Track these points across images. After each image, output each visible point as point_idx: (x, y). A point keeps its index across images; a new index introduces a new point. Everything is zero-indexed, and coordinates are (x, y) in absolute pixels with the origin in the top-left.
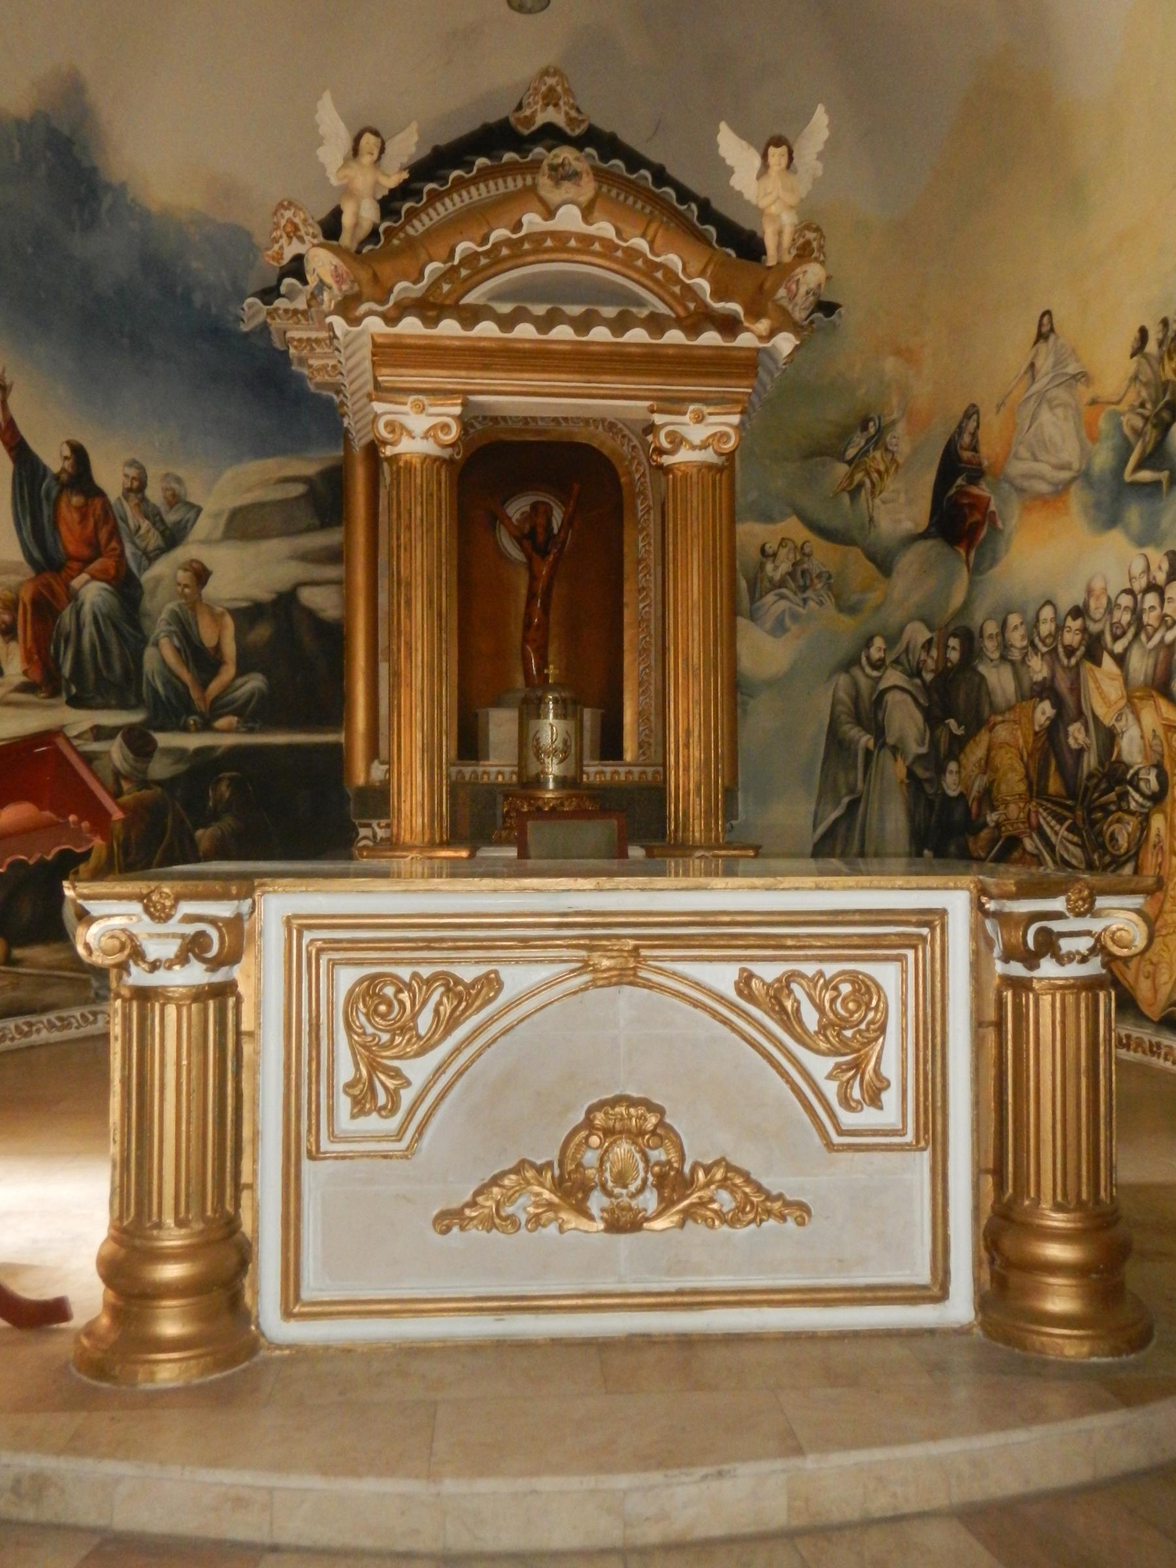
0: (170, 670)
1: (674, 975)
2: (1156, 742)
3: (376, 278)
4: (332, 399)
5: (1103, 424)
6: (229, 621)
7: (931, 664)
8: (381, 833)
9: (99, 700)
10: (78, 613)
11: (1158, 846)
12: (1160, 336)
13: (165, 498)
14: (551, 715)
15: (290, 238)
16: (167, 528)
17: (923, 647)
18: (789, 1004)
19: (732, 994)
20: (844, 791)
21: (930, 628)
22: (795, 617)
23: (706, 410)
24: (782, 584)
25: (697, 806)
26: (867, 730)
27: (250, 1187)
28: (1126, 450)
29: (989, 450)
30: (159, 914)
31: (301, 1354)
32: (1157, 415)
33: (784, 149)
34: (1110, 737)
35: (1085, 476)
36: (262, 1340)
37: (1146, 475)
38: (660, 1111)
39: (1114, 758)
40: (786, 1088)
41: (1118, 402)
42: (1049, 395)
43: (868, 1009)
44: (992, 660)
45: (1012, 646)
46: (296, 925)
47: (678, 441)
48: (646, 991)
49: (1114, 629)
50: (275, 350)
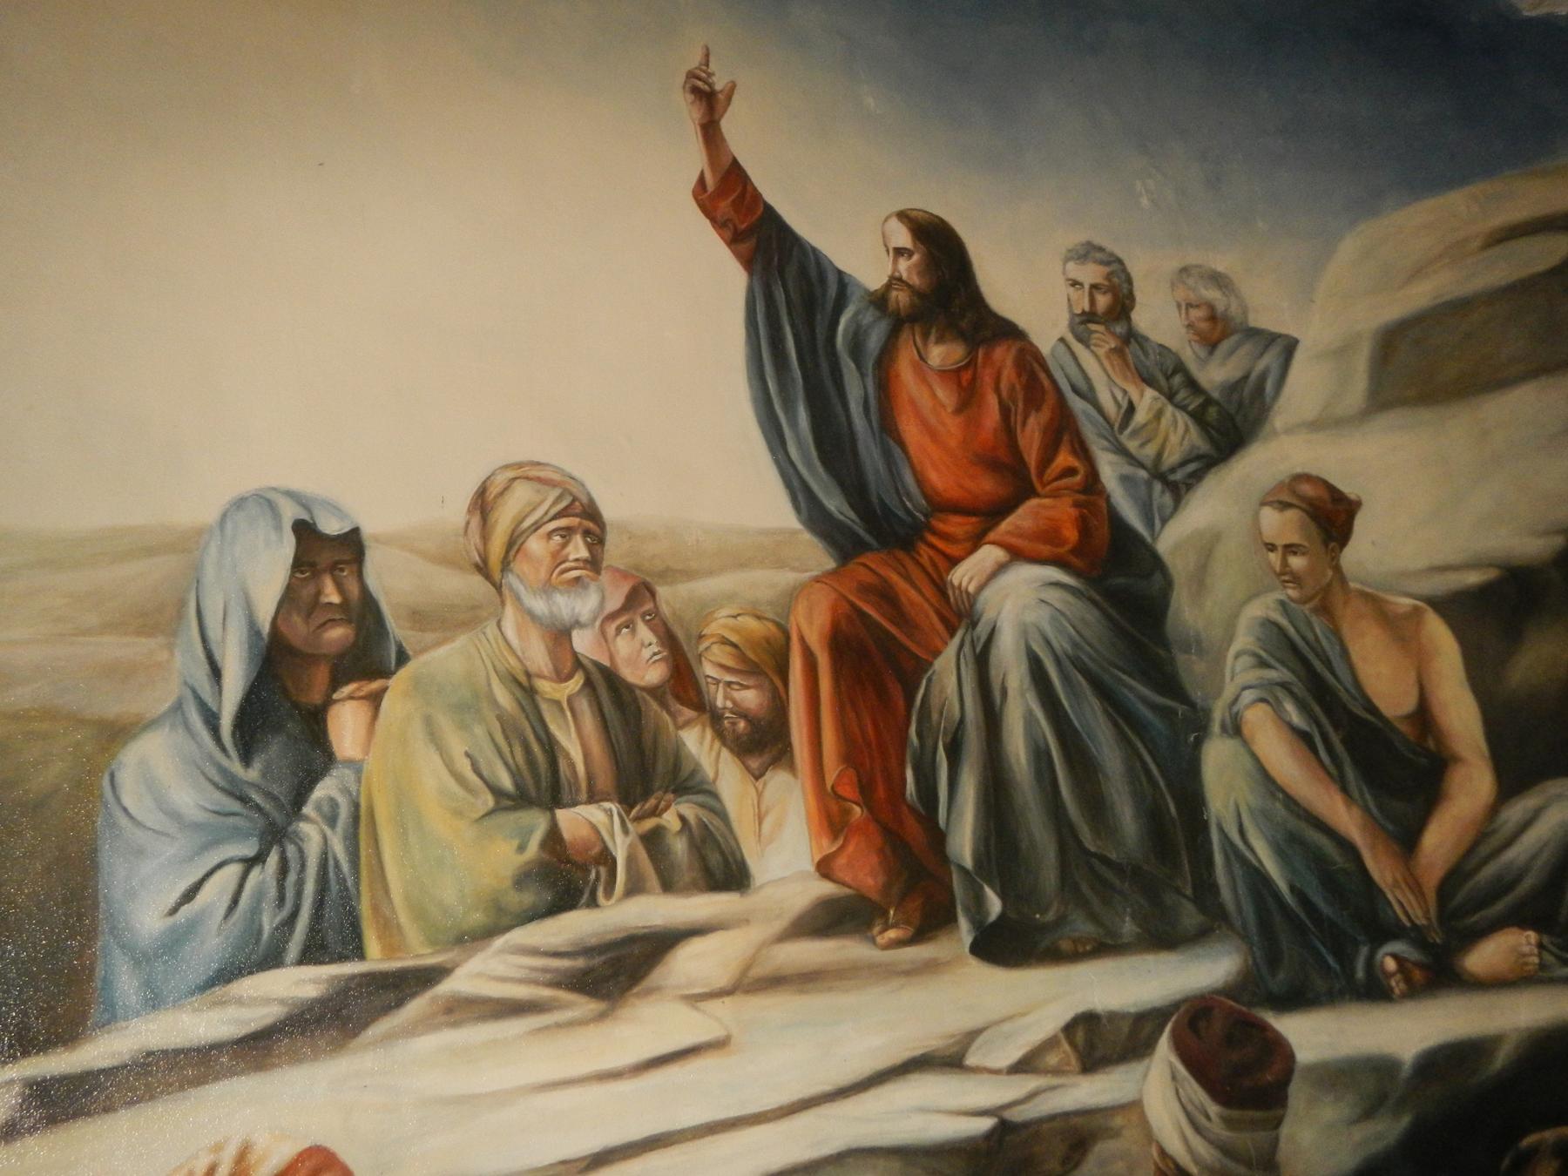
0: (1291, 802)
6: (1440, 636)
9: (1082, 927)
10: (982, 660)
13: (1190, 326)
16: (1209, 401)
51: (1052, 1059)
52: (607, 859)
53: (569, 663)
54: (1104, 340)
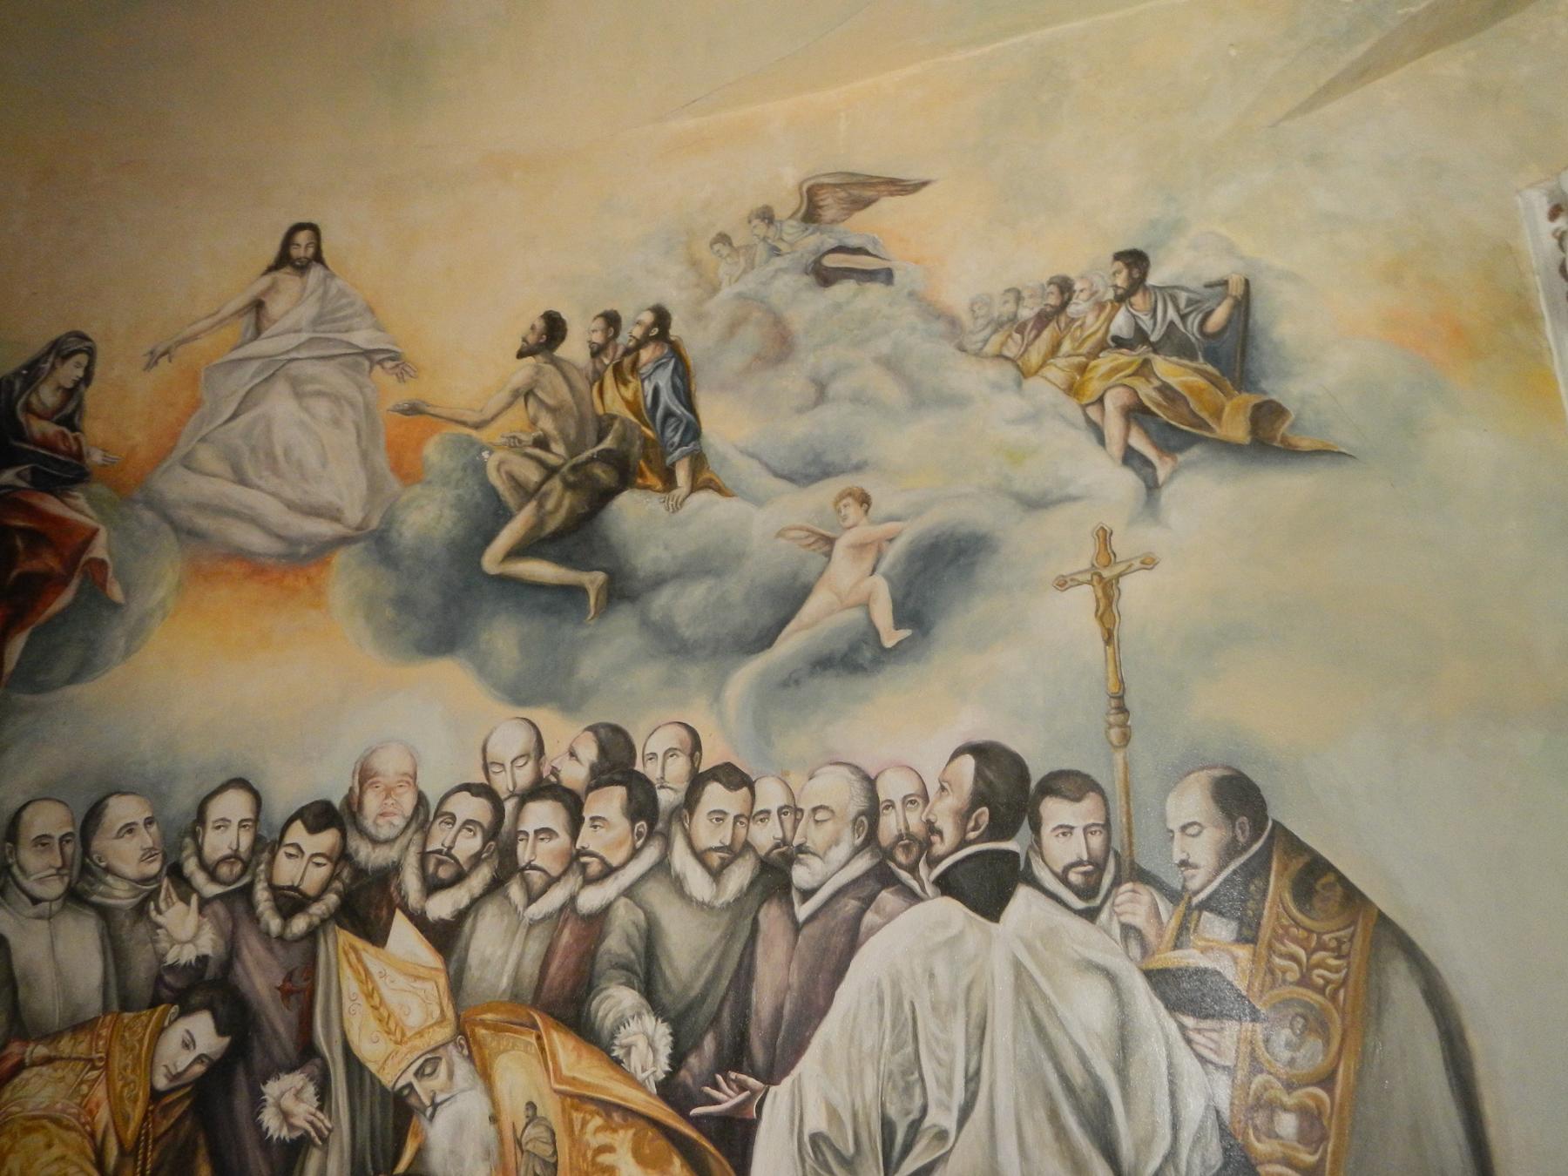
2: (532, 1131)
12: (598, 338)
39: (401, 1167)
41: (478, 426)
42: (294, 368)
44: (36, 901)
45: (108, 870)
49: (431, 869)
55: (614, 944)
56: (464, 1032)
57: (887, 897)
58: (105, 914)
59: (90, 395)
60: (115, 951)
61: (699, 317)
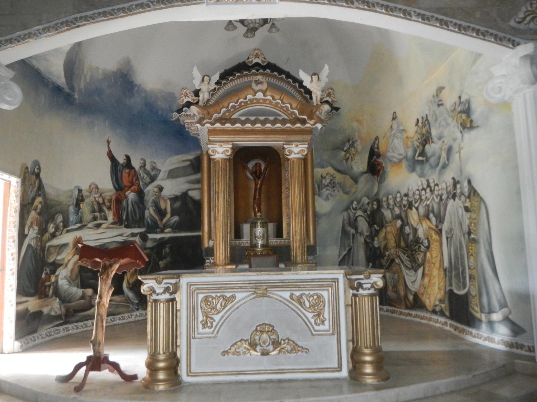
1: (275, 294)
3: (208, 113)
4: (197, 138)
5: (410, 144)
6: (169, 202)
7: (369, 209)
8: (212, 261)
9: (133, 225)
10: (127, 201)
11: (429, 261)
12: (422, 121)
13: (151, 168)
14: (259, 227)
15: (185, 97)
16: (151, 176)
17: (367, 204)
18: (302, 301)
19: (289, 298)
20: (347, 246)
21: (369, 199)
22: (331, 195)
23: (298, 144)
24: (327, 186)
25: (299, 252)
26: (352, 228)
27: (179, 346)
28: (415, 151)
29: (382, 149)
30: (159, 283)
31: (191, 385)
32: (422, 142)
33: (317, 76)
34: (415, 230)
35: (406, 157)
36: (182, 382)
37: (420, 158)
38: (273, 327)
40: (302, 321)
41: (413, 138)
43: (321, 302)
44: (385, 208)
45: (390, 204)
46: (189, 285)
47: (291, 152)
48: (269, 299)
50: (181, 125)
51: (129, 236)
52: (98, 217)
53: (96, 201)
54: (142, 169)
55: (430, 208)
56: (420, 220)
57: (449, 200)
58: (390, 209)
59: (380, 145)
60: (392, 213)
61: (430, 115)
